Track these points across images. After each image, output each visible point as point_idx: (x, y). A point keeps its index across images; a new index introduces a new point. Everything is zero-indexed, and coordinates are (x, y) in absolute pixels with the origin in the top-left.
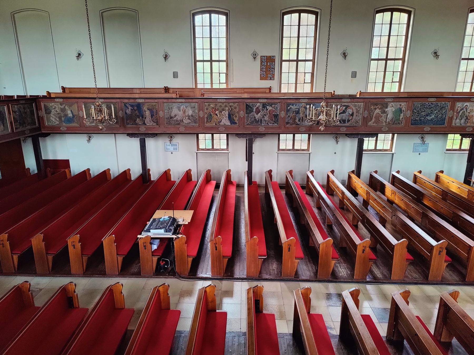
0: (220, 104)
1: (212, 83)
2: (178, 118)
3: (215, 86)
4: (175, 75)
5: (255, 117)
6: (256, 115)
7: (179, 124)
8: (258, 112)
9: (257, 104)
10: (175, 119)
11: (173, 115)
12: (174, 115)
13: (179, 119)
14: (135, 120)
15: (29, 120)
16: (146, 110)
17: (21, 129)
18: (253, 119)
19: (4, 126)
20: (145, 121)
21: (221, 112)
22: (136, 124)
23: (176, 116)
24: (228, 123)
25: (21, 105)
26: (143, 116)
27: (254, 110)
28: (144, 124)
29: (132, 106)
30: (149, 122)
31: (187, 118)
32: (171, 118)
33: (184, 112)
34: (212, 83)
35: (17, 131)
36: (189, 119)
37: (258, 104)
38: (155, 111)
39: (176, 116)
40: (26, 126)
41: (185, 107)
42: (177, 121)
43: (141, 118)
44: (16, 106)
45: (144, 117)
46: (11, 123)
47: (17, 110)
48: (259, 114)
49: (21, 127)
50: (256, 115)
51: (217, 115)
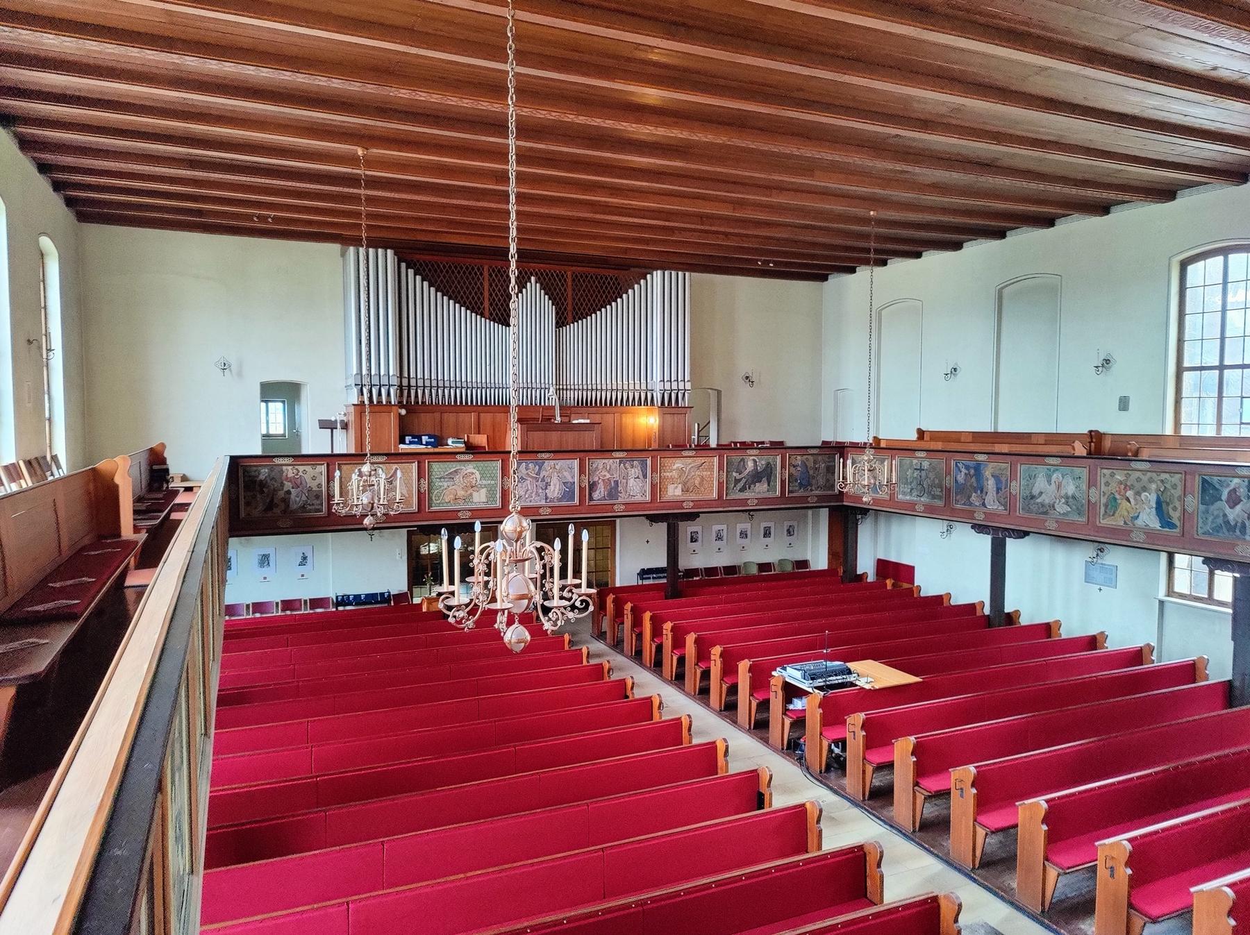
0: (1138, 474)
1: (1219, 424)
2: (1046, 499)
3: (1227, 432)
4: (1124, 404)
5: (1225, 515)
6: (1228, 510)
7: (1046, 513)
8: (1234, 501)
9: (1230, 479)
10: (1039, 500)
11: (1036, 492)
12: (1038, 492)
13: (1047, 501)
14: (970, 497)
15: (821, 481)
16: (990, 477)
17: (801, 493)
18: (1220, 521)
19: (769, 485)
20: (984, 500)
21: (1138, 493)
22: (971, 504)
23: (1041, 493)
24: (1155, 524)
25: (809, 457)
26: (981, 489)
27: (1224, 497)
28: (984, 505)
29: (967, 468)
30: (992, 503)
31: (1063, 500)
32: (1033, 497)
33: (1059, 487)
34: (1219, 424)
35: (791, 495)
36: (1067, 503)
37: (1236, 481)
38: (1003, 479)
39: (1041, 493)
40: (812, 490)
41: (1060, 475)
42: (1043, 506)
43: (979, 492)
44: (799, 458)
45: (985, 490)
46: (783, 482)
47: (800, 463)
48: (1238, 508)
49: (802, 490)
50: (1228, 510)
51: (1129, 501)
